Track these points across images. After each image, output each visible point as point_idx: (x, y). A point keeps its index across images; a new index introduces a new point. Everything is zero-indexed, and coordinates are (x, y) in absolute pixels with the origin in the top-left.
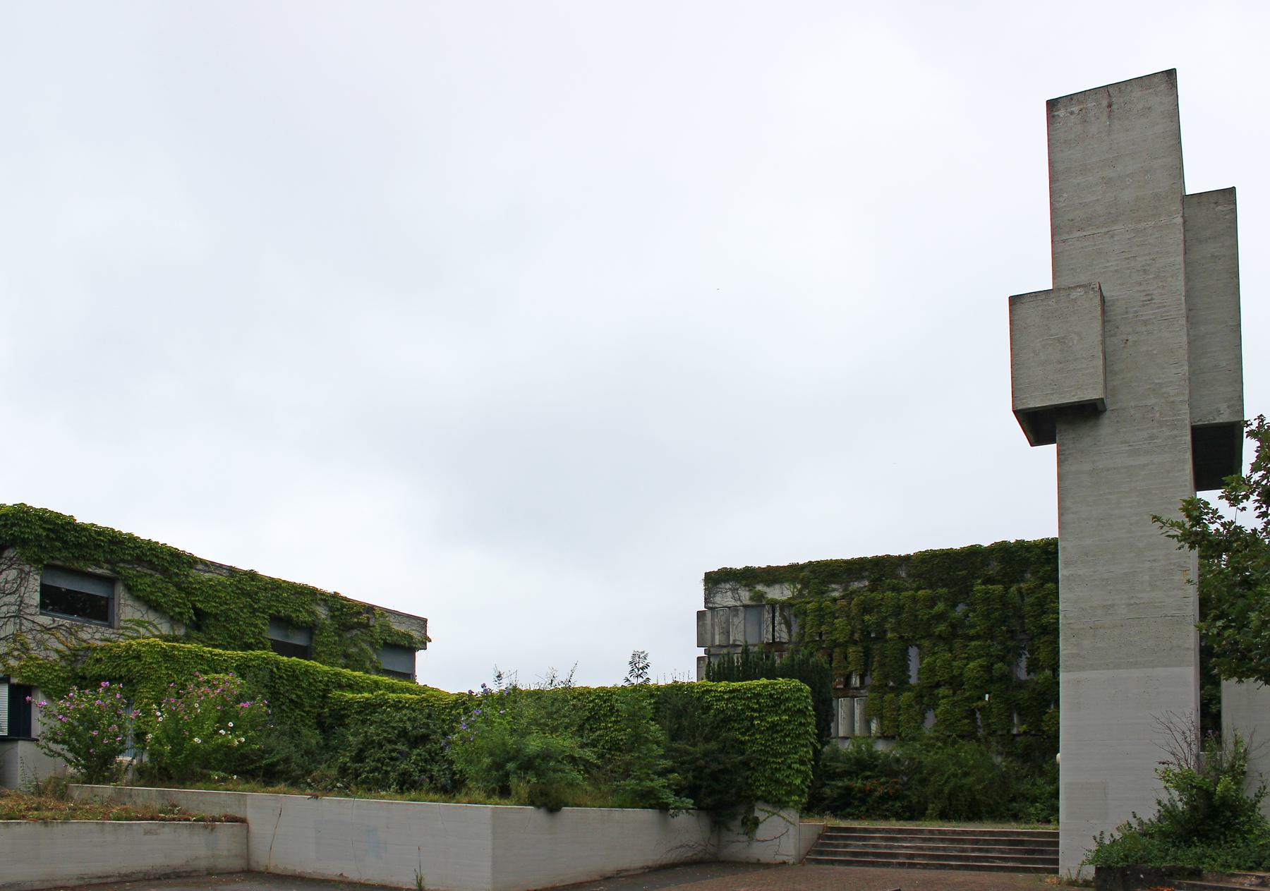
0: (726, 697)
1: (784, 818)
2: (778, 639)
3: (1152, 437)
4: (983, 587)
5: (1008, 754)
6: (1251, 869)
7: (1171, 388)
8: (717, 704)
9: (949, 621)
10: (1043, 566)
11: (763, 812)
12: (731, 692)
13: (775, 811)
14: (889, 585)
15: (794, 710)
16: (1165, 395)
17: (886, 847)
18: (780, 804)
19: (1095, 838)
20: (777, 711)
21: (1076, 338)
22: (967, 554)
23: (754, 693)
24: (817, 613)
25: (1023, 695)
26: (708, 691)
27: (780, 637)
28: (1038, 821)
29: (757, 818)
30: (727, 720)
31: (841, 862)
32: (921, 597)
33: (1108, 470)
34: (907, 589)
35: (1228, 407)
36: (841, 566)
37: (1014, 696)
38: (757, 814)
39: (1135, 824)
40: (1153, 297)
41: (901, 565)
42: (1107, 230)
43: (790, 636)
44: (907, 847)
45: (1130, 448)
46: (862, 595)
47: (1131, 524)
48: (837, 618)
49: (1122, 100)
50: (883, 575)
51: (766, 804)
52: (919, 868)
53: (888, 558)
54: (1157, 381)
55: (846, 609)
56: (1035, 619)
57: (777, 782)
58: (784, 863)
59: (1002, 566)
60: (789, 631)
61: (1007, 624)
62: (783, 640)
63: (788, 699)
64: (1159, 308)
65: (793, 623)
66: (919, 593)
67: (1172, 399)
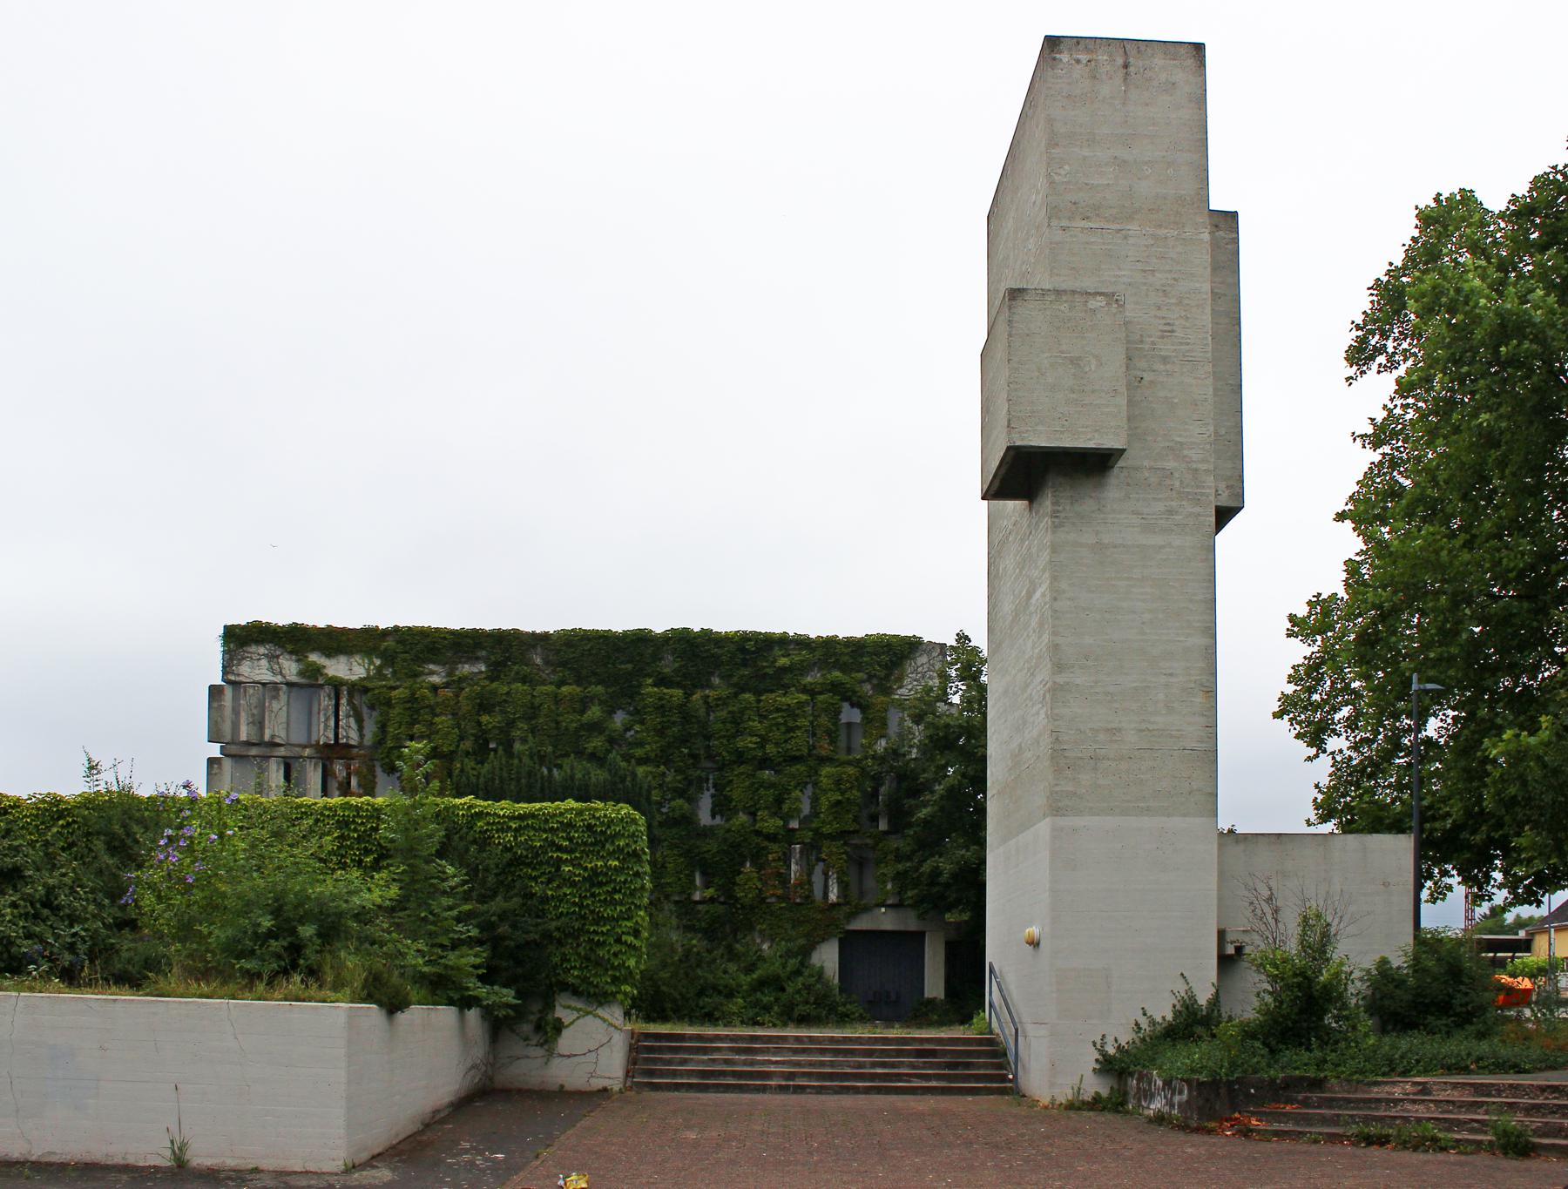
0: (514, 826)
1: (604, 1020)
2: (345, 740)
3: (1171, 512)
4: (656, 689)
5: (689, 928)
6: (1405, 1073)
7: (1194, 451)
8: (499, 837)
9: (607, 733)
10: (738, 669)
11: (569, 1011)
12: (521, 817)
13: (590, 1009)
14: (517, 673)
15: (628, 852)
16: (1187, 459)
17: (745, 1063)
18: (601, 998)
19: (1094, 1044)
20: (598, 852)
21: (1094, 363)
22: (632, 641)
23: (562, 823)
24: (409, 705)
25: (711, 846)
26: (480, 815)
27: (348, 737)
28: (742, 1022)
29: (559, 1020)
30: (517, 861)
31: (689, 1087)
32: (565, 696)
33: (1115, 547)
34: (543, 683)
35: (1227, 487)
36: (445, 638)
37: (697, 847)
38: (560, 1013)
39: (1144, 1023)
40: (1175, 328)
41: (534, 647)
42: (1119, 227)
43: (362, 736)
44: (777, 1062)
45: (1143, 521)
46: (476, 684)
47: (1143, 623)
48: (437, 716)
49: (1141, 63)
50: (509, 659)
51: (574, 997)
52: (810, 1093)
53: (515, 635)
54: (1178, 439)
55: (452, 703)
56: (728, 741)
57: (598, 964)
58: (605, 1090)
59: (683, 663)
60: (361, 729)
61: (689, 744)
62: (352, 742)
63: (617, 835)
64: (1181, 344)
65: (366, 717)
66: (564, 689)
67: (1195, 466)
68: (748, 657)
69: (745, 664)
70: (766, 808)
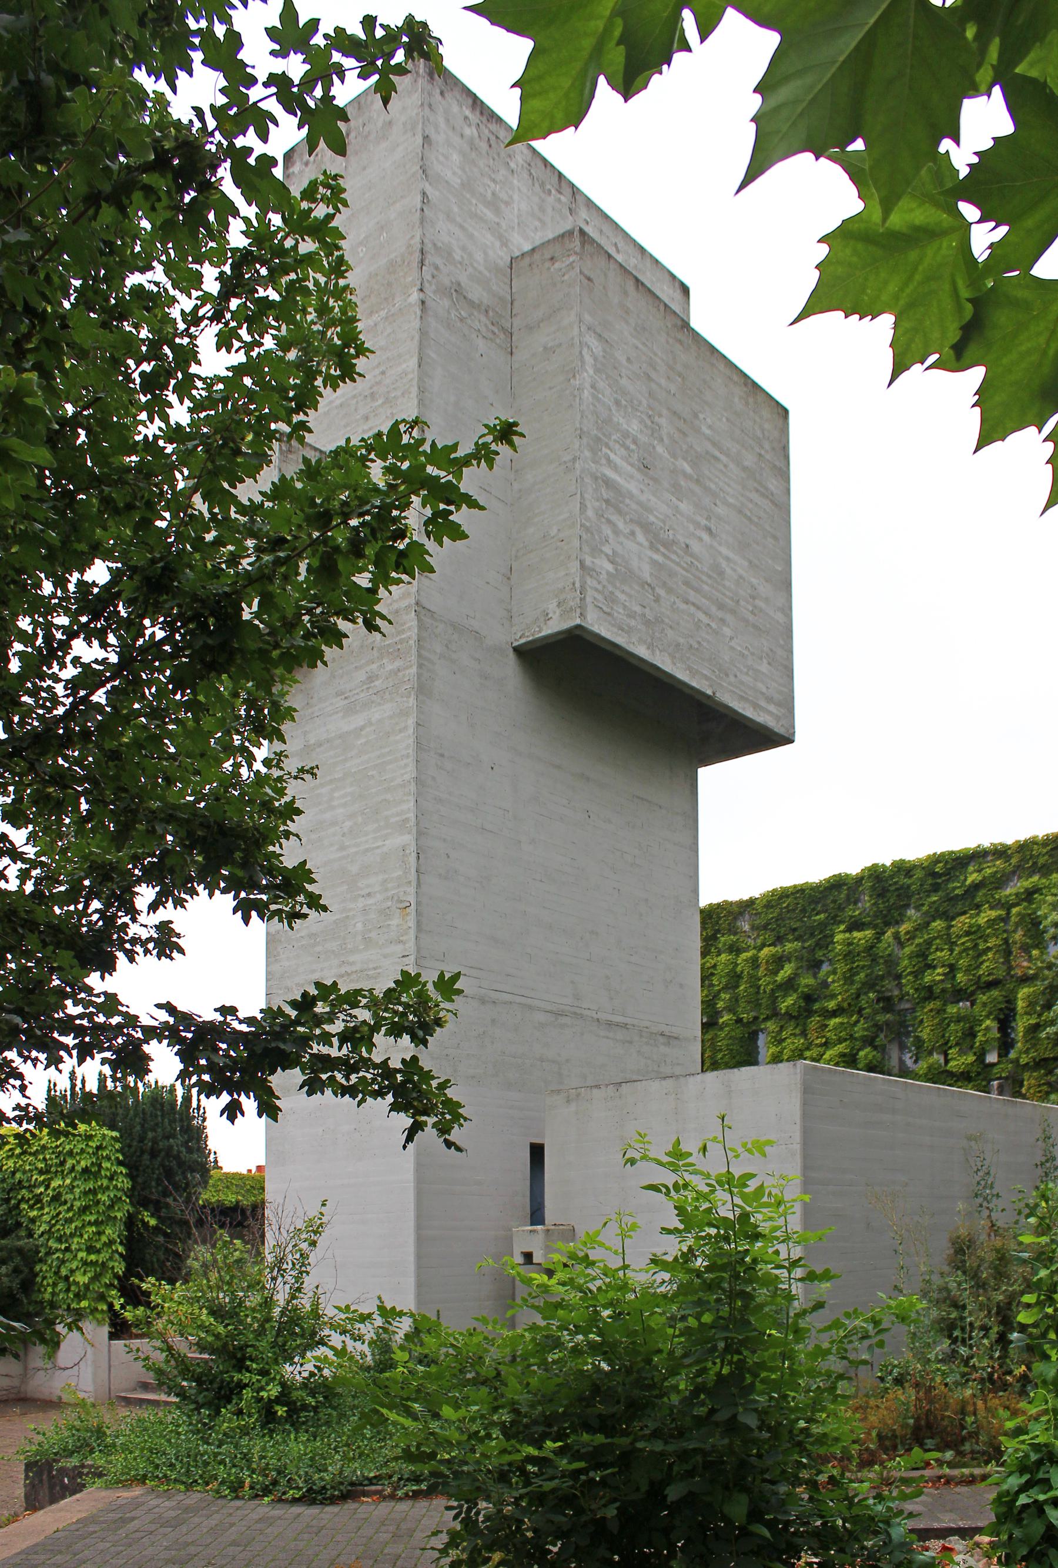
10: (928, 896)
14: (725, 944)
22: (826, 889)
34: (746, 950)
50: (718, 931)
56: (916, 977)
68: (939, 881)
69: (936, 888)
70: (957, 1044)
